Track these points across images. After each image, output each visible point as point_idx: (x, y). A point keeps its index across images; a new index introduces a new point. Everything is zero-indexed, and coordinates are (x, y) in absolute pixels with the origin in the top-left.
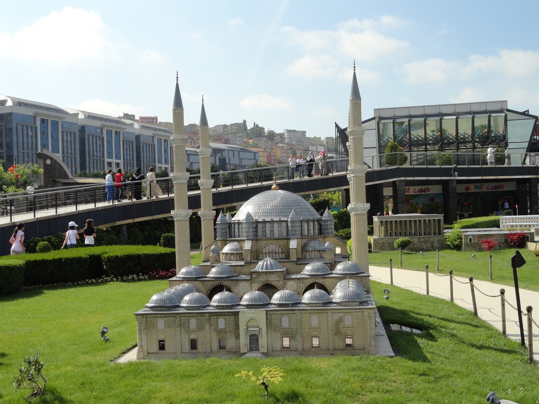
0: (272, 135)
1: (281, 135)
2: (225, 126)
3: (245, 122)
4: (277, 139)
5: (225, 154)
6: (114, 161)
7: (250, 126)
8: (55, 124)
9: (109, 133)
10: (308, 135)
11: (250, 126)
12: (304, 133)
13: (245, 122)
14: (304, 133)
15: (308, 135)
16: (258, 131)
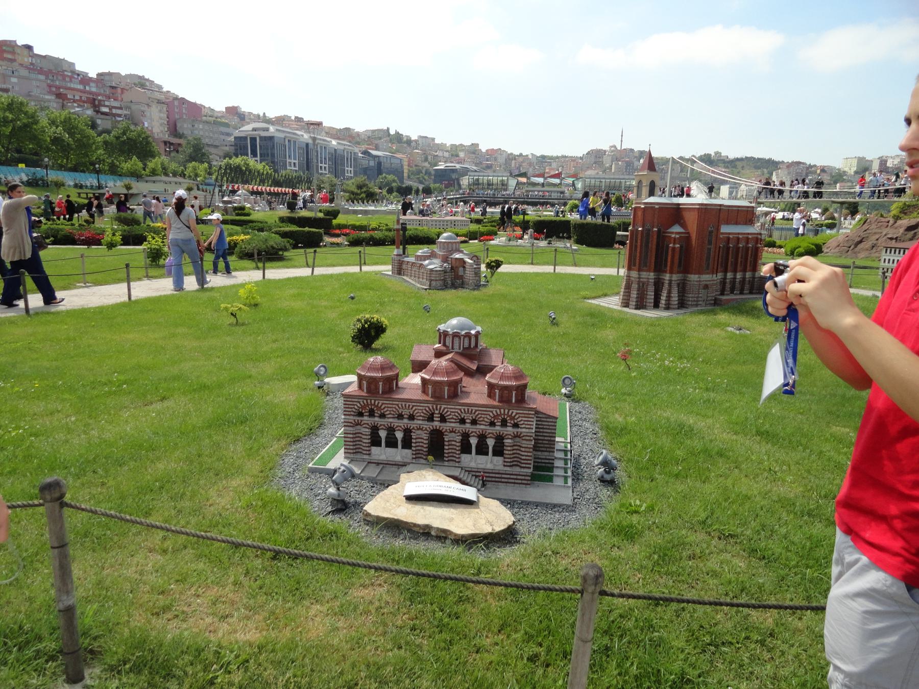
0: (409, 142)
1: (416, 141)
2: (373, 131)
3: (388, 129)
4: (413, 144)
5: (381, 160)
6: (323, 165)
7: (392, 132)
8: (295, 142)
9: (321, 147)
10: (437, 141)
11: (392, 132)
12: (433, 139)
13: (388, 129)
14: (433, 139)
15: (437, 141)
16: (398, 137)
